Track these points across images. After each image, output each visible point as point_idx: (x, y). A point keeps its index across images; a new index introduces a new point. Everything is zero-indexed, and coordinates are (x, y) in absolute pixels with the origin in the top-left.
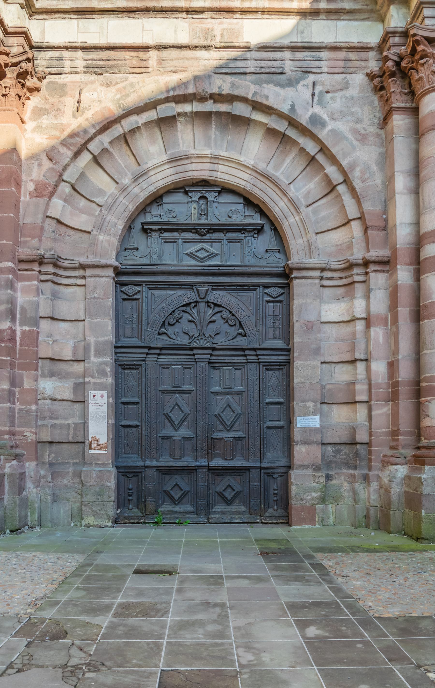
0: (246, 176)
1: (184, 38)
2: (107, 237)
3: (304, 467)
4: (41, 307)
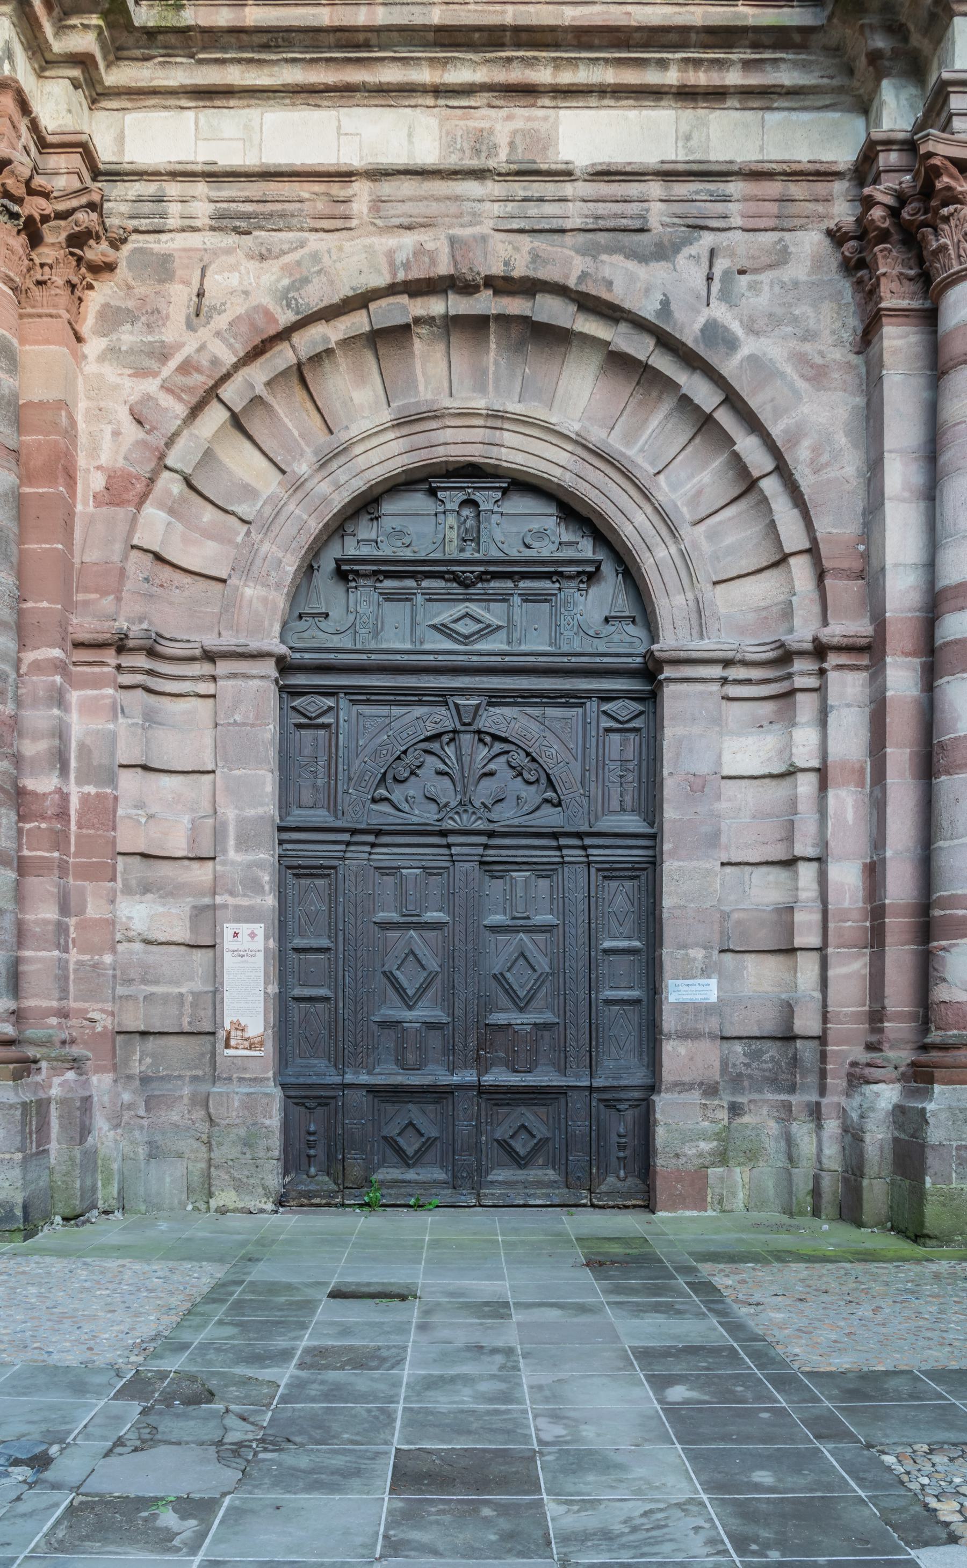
0: (563, 457)
1: (428, 153)
2: (260, 591)
3: (682, 1086)
4: (121, 744)
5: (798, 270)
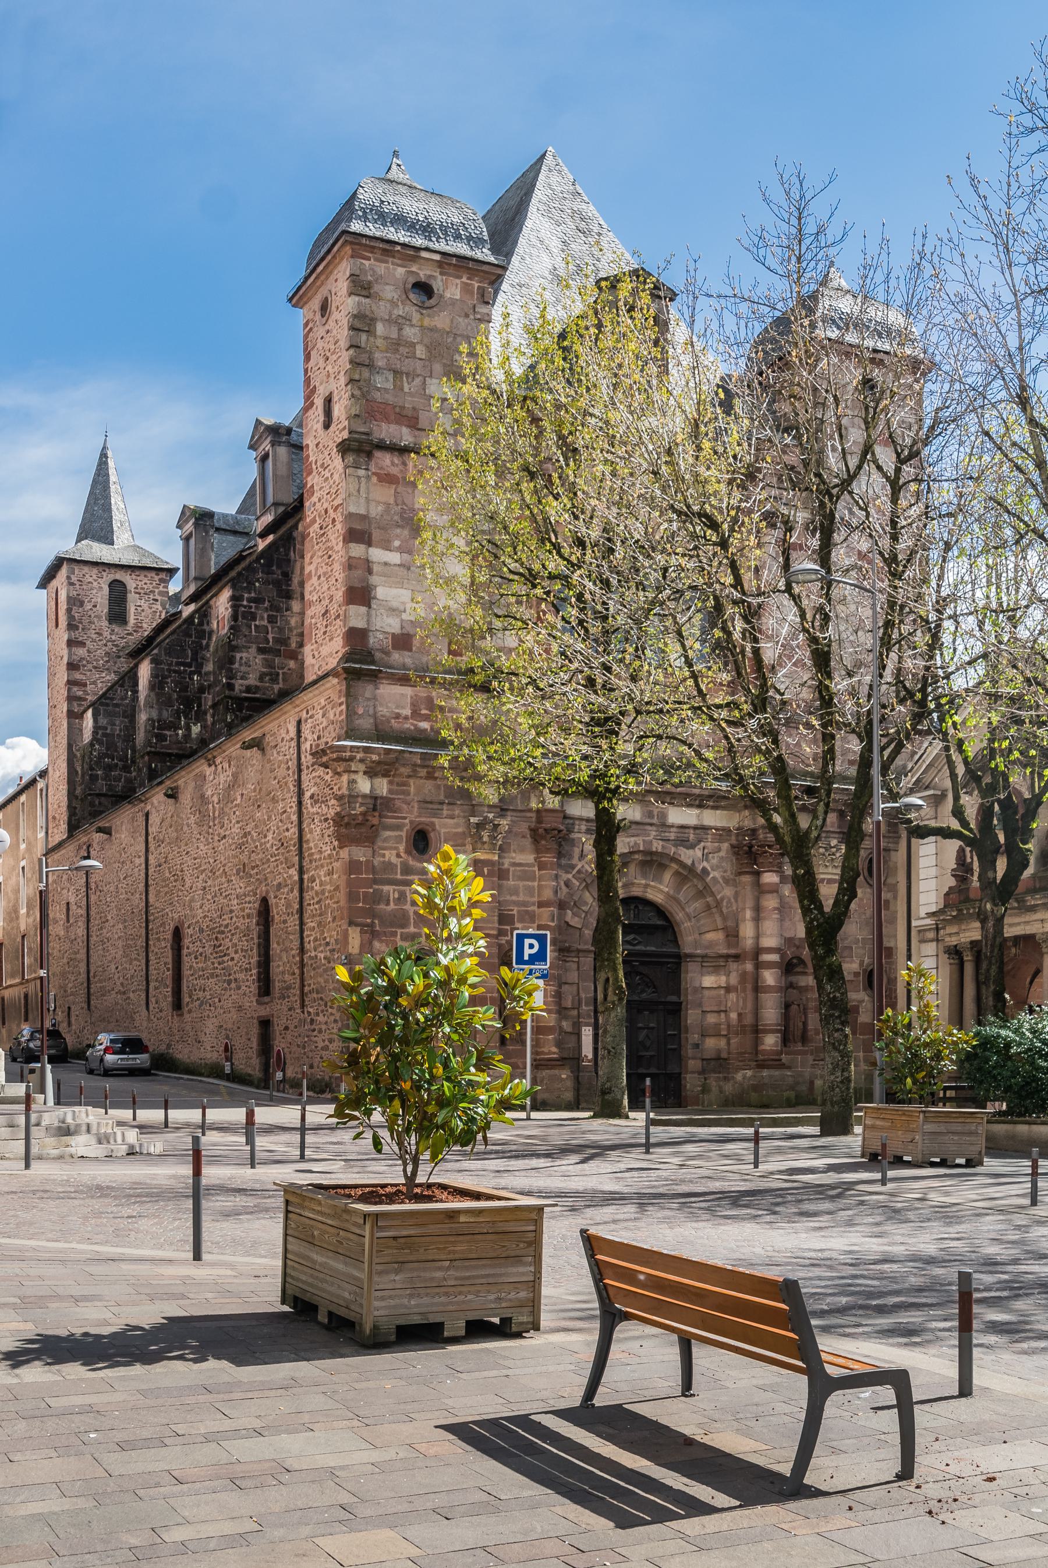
5: (722, 854)
